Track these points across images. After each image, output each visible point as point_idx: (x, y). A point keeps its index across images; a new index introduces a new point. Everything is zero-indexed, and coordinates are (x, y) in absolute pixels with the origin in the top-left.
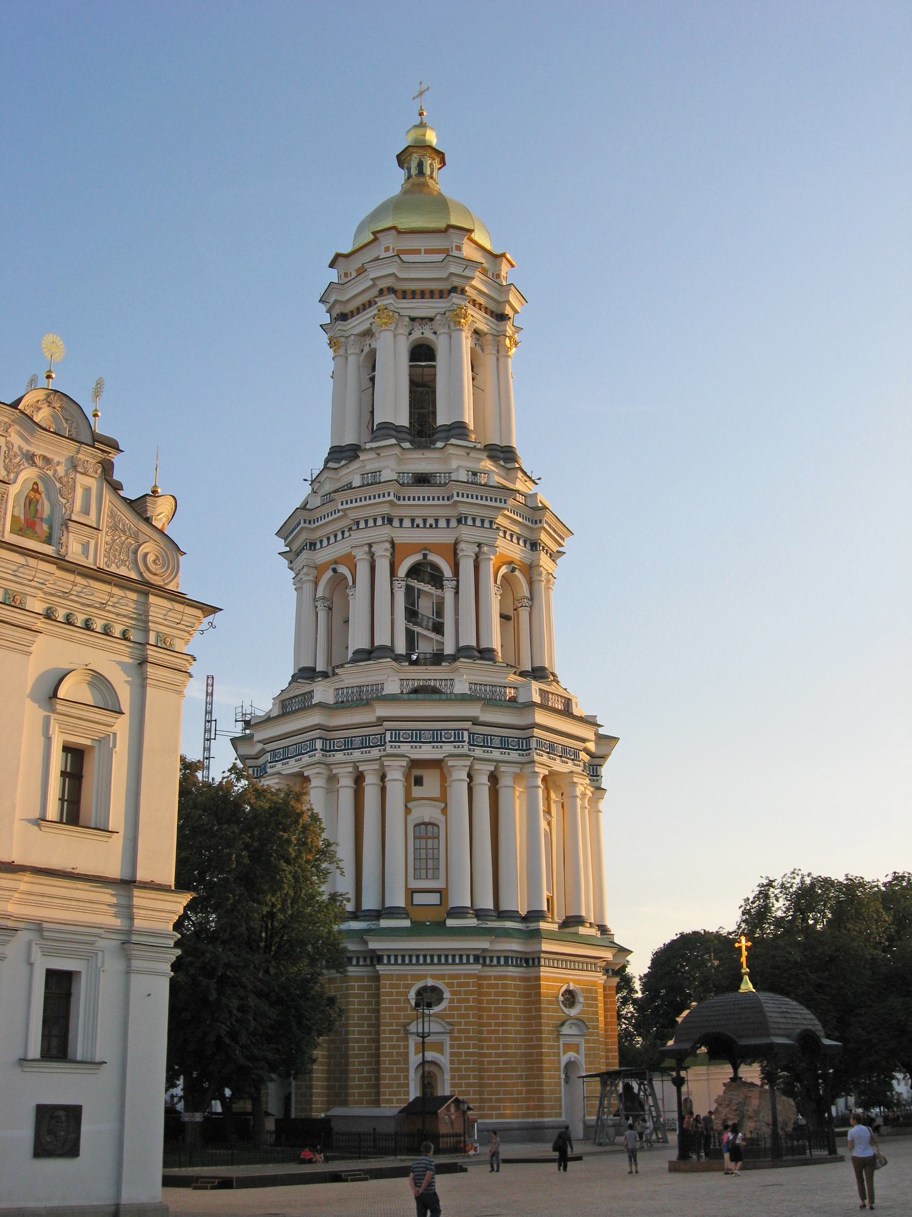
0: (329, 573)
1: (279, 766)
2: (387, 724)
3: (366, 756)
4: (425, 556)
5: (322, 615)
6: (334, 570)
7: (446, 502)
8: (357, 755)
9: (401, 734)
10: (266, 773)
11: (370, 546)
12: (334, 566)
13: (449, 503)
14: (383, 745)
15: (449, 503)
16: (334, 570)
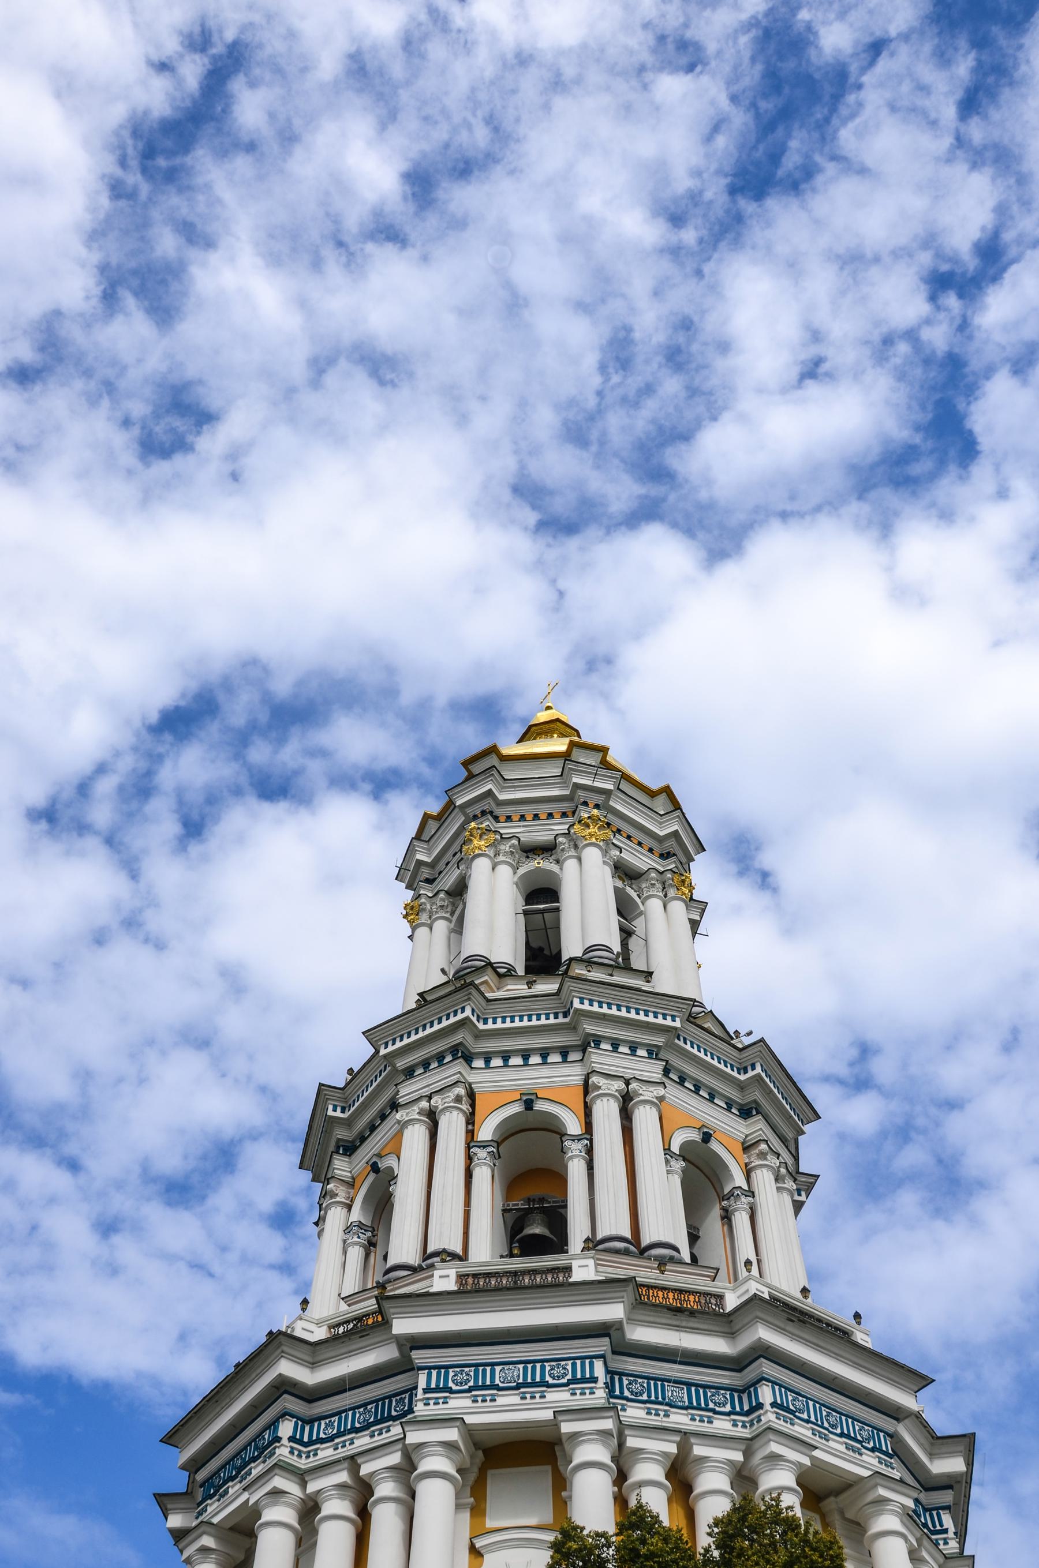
0: (517, 1108)
1: (458, 1404)
2: (767, 1368)
3: (705, 1428)
4: (707, 1137)
5: (483, 1175)
6: (529, 1105)
7: (735, 1074)
8: (679, 1419)
9: (790, 1398)
10: (411, 1411)
11: (627, 1083)
12: (533, 1097)
13: (742, 1077)
14: (747, 1414)
15: (742, 1077)
16: (529, 1105)
